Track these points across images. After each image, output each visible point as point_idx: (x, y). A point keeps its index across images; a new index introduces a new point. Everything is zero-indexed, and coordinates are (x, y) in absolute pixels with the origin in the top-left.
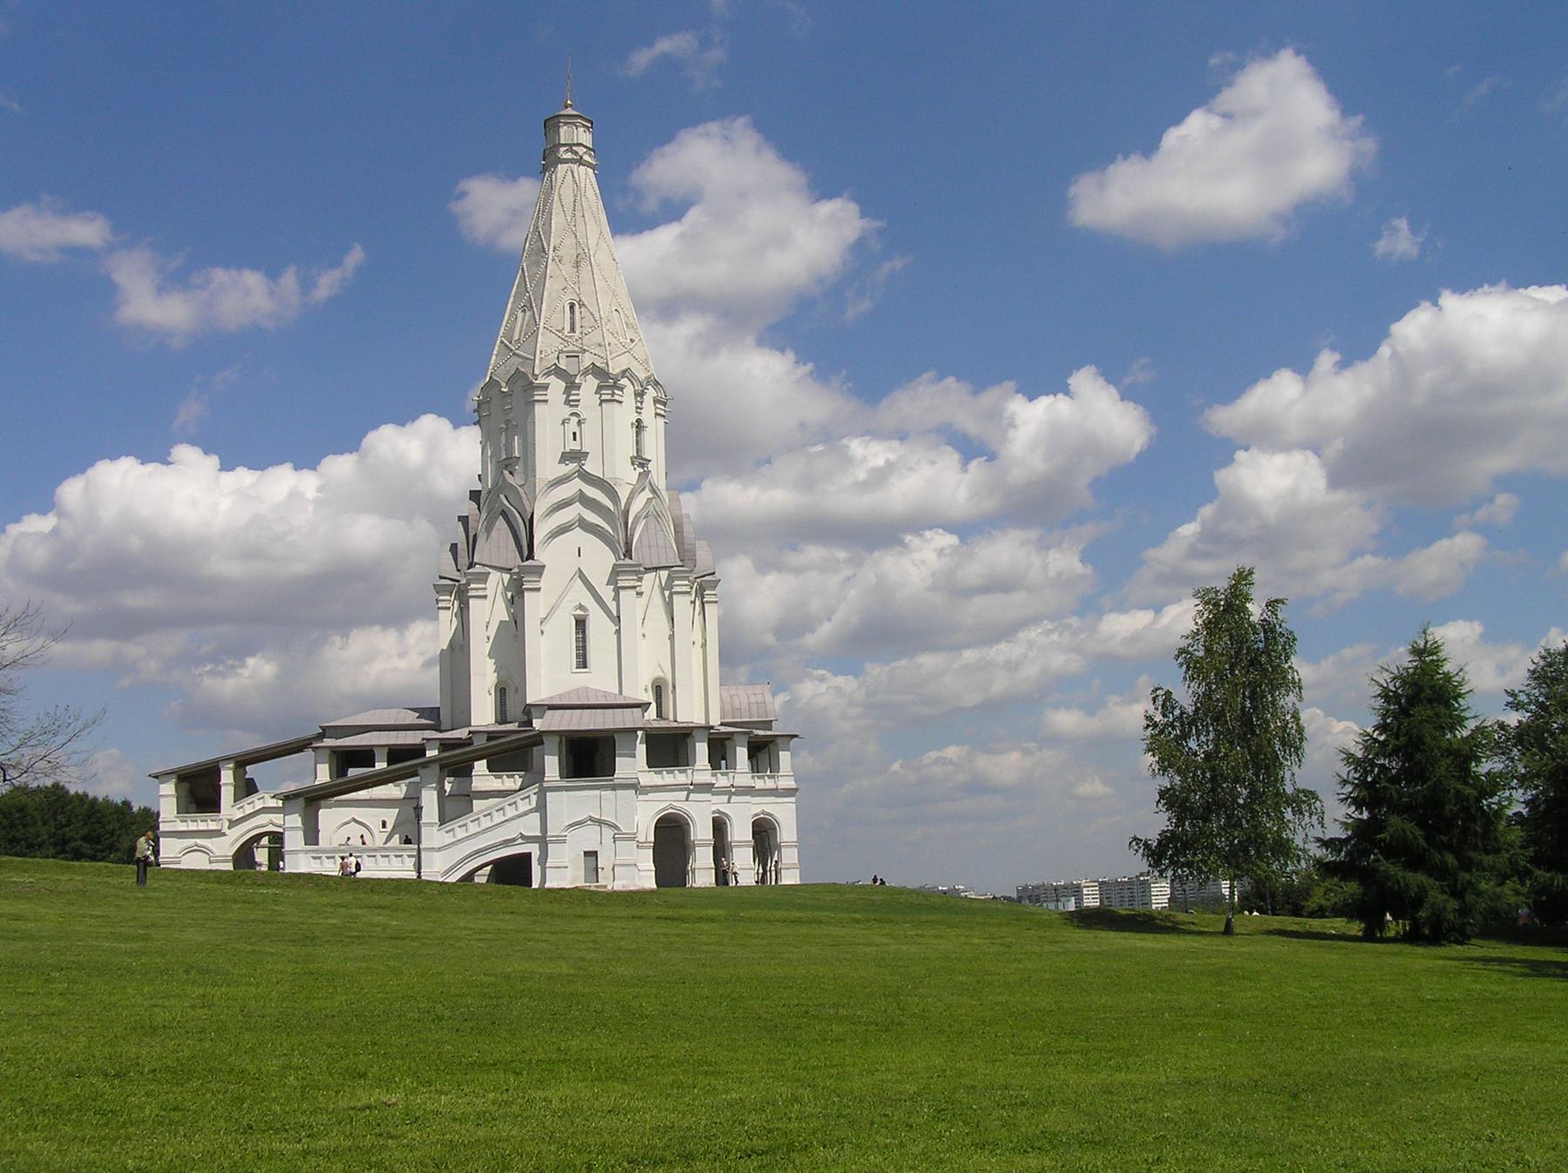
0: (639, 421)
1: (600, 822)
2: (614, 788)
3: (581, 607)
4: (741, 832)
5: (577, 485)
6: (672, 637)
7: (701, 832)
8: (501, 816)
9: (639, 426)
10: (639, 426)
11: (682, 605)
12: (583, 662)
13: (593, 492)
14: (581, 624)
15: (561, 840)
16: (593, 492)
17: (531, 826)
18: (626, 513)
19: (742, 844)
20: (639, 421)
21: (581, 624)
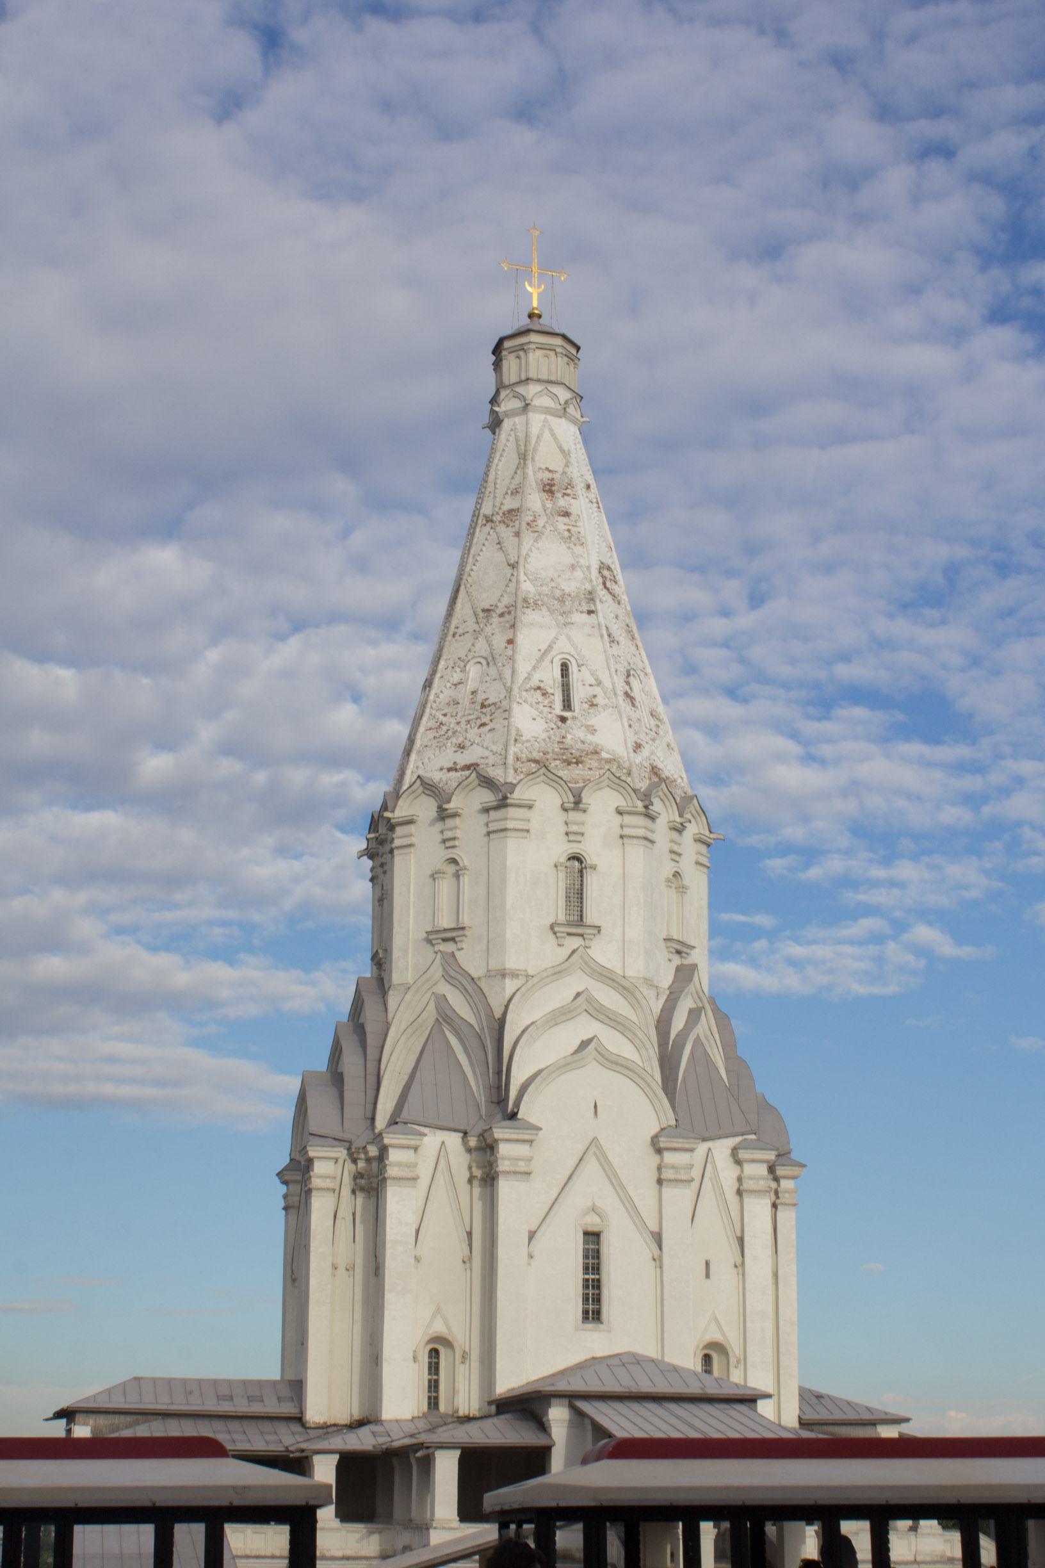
0: (677, 874)
3: (594, 1209)
11: (758, 1210)
12: (593, 1311)
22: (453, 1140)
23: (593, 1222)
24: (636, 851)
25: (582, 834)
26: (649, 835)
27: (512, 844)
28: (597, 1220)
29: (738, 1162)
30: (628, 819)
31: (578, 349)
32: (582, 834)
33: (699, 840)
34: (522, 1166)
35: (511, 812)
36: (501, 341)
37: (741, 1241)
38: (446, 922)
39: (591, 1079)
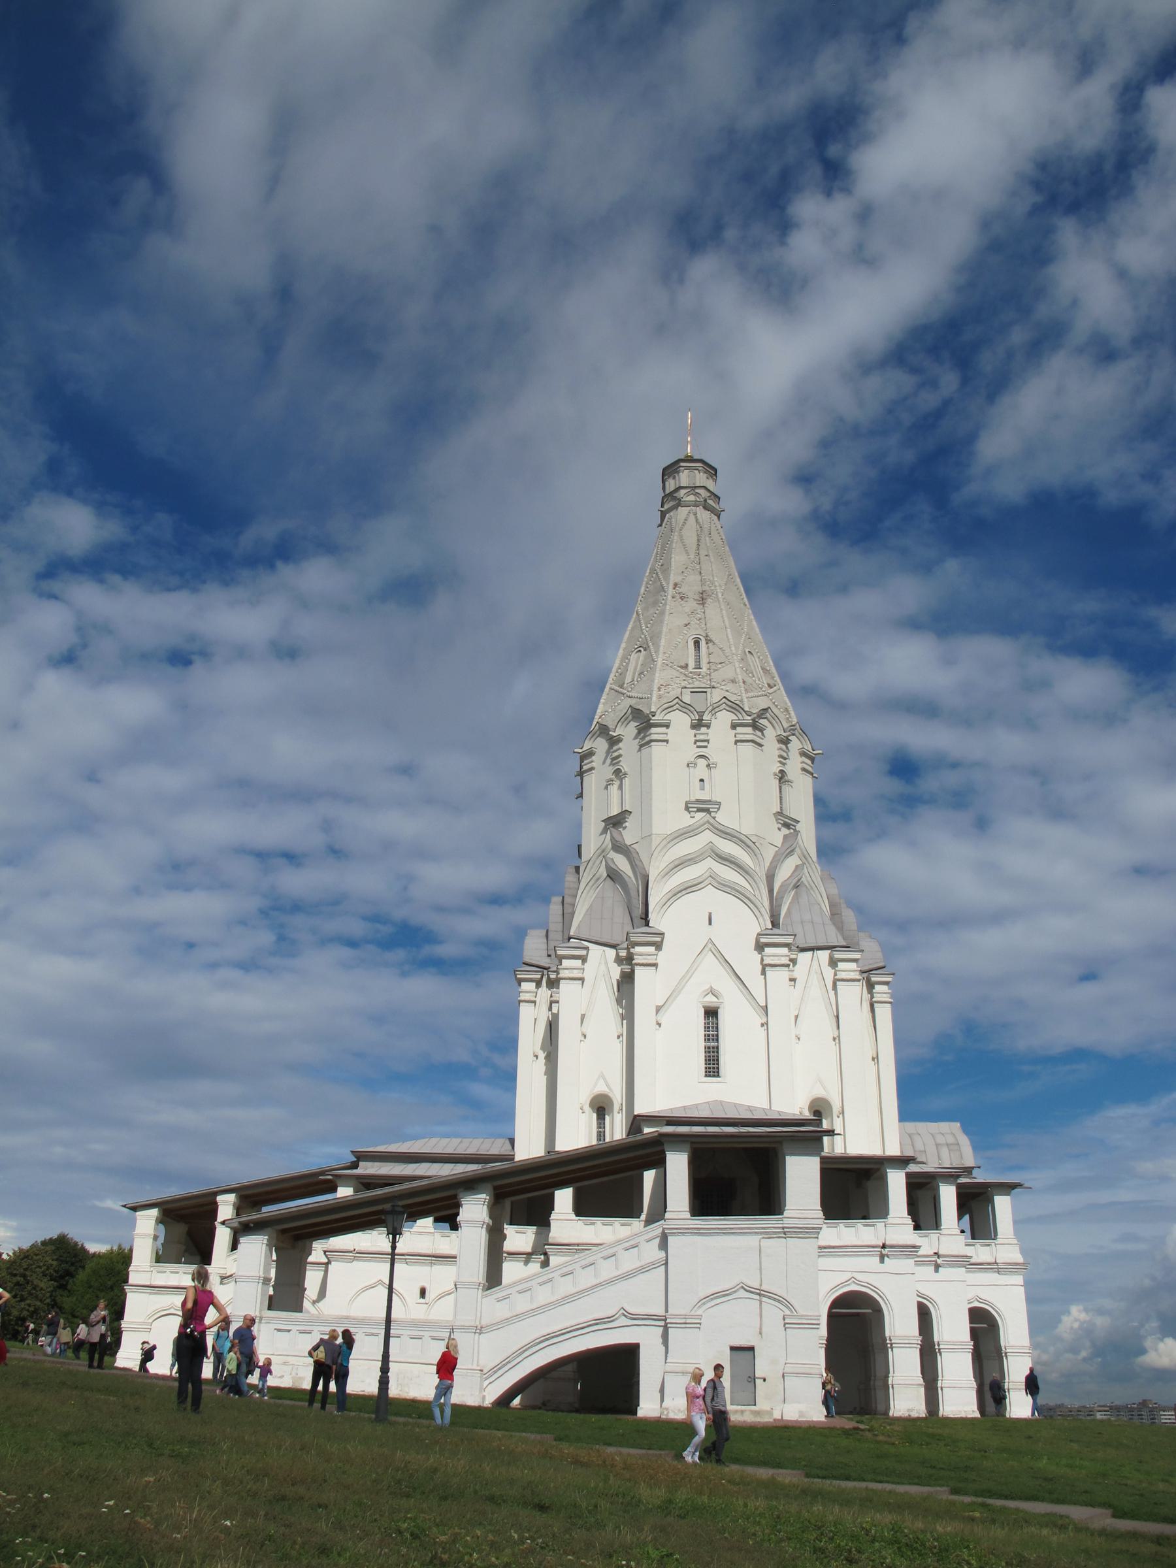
1: (761, 1293)
2: (785, 1233)
3: (712, 992)
4: (953, 1330)
5: (707, 837)
6: (837, 1039)
7: (900, 1325)
8: (595, 1282)
9: (782, 777)
10: (782, 777)
12: (713, 1068)
13: (728, 847)
14: (711, 1013)
15: (691, 1323)
16: (728, 847)
17: (644, 1295)
18: (770, 878)
19: (955, 1347)
20: (782, 771)
21: (711, 1013)
22: (611, 953)
23: (711, 1000)
24: (747, 750)
25: (708, 741)
26: (759, 740)
27: (656, 749)
28: (715, 999)
29: (833, 963)
30: (739, 729)
31: (716, 470)
32: (708, 741)
33: (803, 754)
34: (651, 960)
35: (653, 730)
36: (664, 470)
37: (837, 1017)
38: (615, 811)
39: (710, 898)
